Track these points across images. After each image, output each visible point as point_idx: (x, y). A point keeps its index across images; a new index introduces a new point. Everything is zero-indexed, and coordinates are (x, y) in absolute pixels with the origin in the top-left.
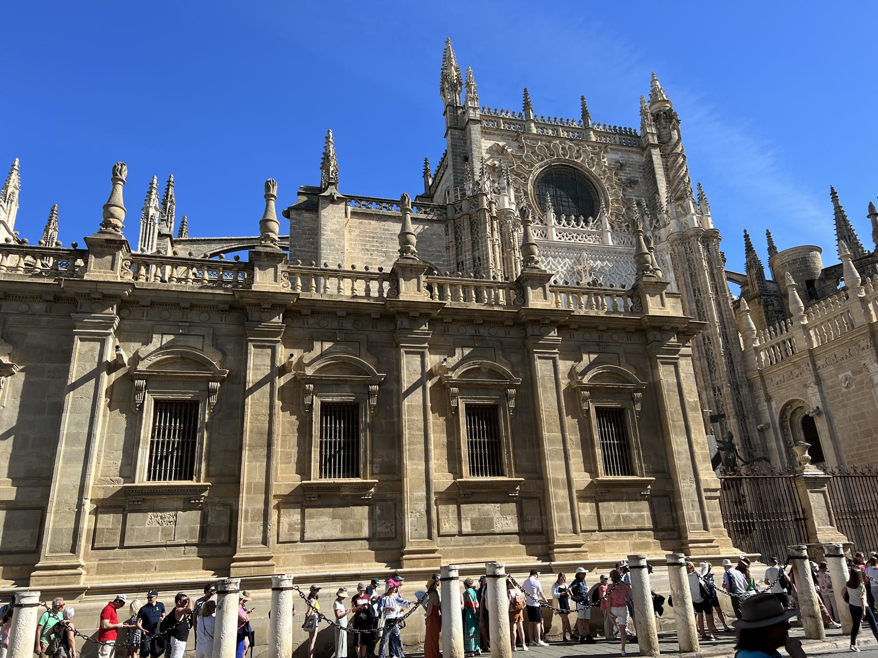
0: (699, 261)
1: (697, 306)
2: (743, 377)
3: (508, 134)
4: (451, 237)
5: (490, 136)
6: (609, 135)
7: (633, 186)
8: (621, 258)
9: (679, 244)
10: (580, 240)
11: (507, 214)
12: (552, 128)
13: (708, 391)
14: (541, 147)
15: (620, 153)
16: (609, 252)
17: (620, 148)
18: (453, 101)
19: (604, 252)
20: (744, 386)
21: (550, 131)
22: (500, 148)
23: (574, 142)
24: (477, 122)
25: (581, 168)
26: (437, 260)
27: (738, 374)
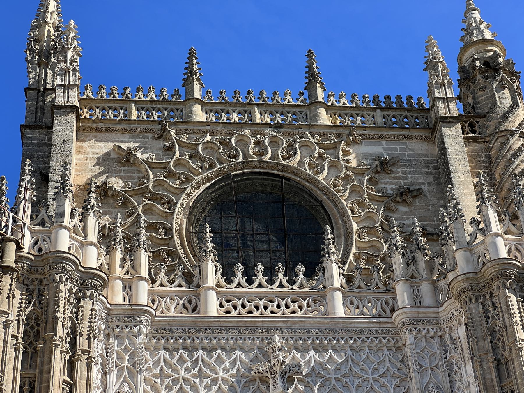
0: (509, 330)
3: (143, 127)
5: (108, 135)
6: (361, 113)
7: (409, 200)
8: (364, 341)
9: (470, 300)
10: (272, 312)
12: (238, 109)
14: (209, 145)
15: (384, 142)
16: (335, 331)
17: (383, 133)
18: (39, 81)
19: (322, 332)
21: (235, 114)
22: (124, 154)
23: (281, 130)
24: (68, 109)
25: (296, 175)
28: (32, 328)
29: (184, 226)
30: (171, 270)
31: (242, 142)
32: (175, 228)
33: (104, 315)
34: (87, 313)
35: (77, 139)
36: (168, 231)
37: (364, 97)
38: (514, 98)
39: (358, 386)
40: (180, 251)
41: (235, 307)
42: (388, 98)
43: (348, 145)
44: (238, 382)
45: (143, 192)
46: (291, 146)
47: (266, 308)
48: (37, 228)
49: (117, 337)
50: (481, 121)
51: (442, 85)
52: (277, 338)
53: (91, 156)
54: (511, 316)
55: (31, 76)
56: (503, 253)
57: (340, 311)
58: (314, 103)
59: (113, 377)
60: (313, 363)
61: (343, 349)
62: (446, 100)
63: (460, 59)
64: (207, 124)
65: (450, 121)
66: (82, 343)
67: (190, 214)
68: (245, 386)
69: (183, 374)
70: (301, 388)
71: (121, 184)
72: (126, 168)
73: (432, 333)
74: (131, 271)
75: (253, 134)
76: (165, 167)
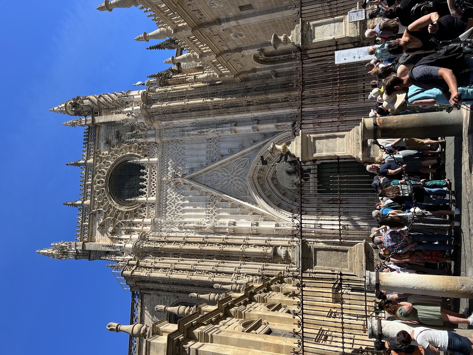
0: (163, 108)
1: (194, 111)
2: (240, 85)
3: (91, 221)
4: (152, 292)
8: (166, 153)
10: (155, 180)
11: (136, 248)
12: (86, 189)
13: (251, 109)
15: (100, 142)
16: (162, 161)
17: (97, 142)
18: (73, 255)
19: (162, 165)
20: (246, 85)
23: (94, 175)
24: (84, 245)
25: (110, 171)
27: (238, 88)
28: (157, 255)
30: (141, 212)
32: (126, 210)
34: (153, 238)
37: (84, 147)
38: (86, 99)
39: (179, 155)
40: (134, 208)
41: (153, 192)
42: (84, 140)
43: (100, 154)
44: (177, 191)
45: (114, 221)
46: (100, 172)
47: (154, 182)
48: (124, 254)
49: (161, 228)
50: (94, 110)
51: (80, 121)
53: (101, 238)
54: (159, 107)
55: (71, 258)
56: (139, 107)
57: (156, 159)
58: (85, 164)
59: (173, 229)
61: (168, 159)
62: (86, 120)
63: (71, 115)
64: (91, 199)
65: (93, 120)
66: (163, 239)
67: (122, 205)
68: (178, 189)
69: (174, 208)
70: (179, 172)
71: (111, 227)
73: (163, 132)
74: (140, 224)
75: (96, 184)
76: (105, 213)
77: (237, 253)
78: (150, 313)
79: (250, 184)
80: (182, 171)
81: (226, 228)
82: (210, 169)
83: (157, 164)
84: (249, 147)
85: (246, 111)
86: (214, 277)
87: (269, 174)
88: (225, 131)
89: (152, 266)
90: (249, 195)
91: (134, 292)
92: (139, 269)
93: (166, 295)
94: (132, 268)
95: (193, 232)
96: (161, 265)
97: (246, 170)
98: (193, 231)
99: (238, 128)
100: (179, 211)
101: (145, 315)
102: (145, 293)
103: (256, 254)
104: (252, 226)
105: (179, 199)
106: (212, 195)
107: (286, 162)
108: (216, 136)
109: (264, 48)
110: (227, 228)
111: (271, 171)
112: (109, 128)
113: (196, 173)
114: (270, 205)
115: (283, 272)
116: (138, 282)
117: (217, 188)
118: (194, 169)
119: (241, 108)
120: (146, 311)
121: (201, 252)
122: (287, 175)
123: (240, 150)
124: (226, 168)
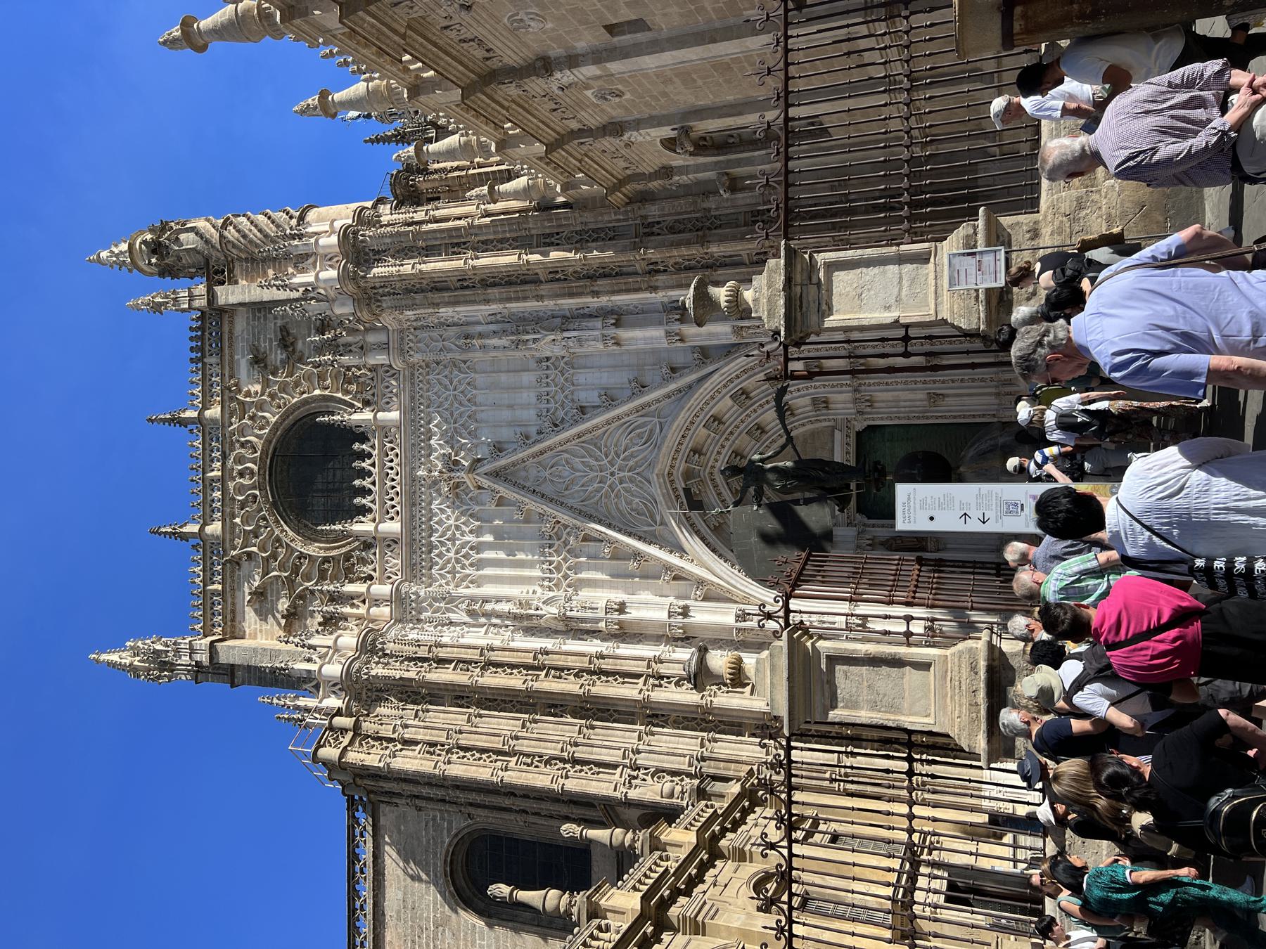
0: (403, 277)
1: (494, 285)
2: (627, 212)
3: (229, 580)
6: (208, 377)
7: (291, 339)
9: (379, 306)
11: (351, 680)
13: (658, 284)
14: (244, 520)
15: (236, 357)
17: (227, 357)
18: (189, 671)
19: (414, 433)
20: (642, 212)
21: (214, 495)
23: (227, 452)
24: (213, 650)
25: (270, 442)
26: (442, 832)
27: (619, 220)
28: (409, 697)
29: (322, 545)
30: (363, 561)
31: (240, 489)
33: (400, 625)
35: (243, 638)
36: (326, 560)
37: (192, 372)
39: (461, 404)
40: (344, 550)
41: (393, 507)
42: (192, 349)
43: (240, 391)
44: (458, 507)
45: (291, 583)
46: (243, 445)
47: (393, 480)
48: (321, 693)
50: (212, 263)
51: (175, 300)
52: (420, 473)
53: (258, 626)
54: (392, 275)
55: (184, 678)
56: (332, 273)
57: (394, 415)
58: (200, 420)
59: (453, 616)
60: (441, 442)
61: (429, 414)
62: (191, 297)
63: (151, 274)
64: (224, 521)
65: (211, 296)
66: (423, 652)
68: (461, 502)
69: (452, 555)
70: (463, 454)
71: (284, 599)
72: (269, 595)
73: (411, 337)
74: (362, 599)
75: (233, 479)
76: (267, 560)
77: (628, 703)
78: (399, 854)
79: (663, 496)
80: (470, 450)
81: (598, 620)
82: (550, 448)
83: (399, 428)
84: (660, 386)
85: (646, 289)
86: (567, 777)
87: (716, 461)
88: (587, 340)
89: (395, 736)
90: (661, 524)
91: (353, 797)
92: (361, 745)
93: (440, 810)
94: (341, 739)
95: (507, 627)
96: (420, 735)
97: (652, 452)
98: (507, 622)
99: (624, 334)
100: (467, 563)
101: (387, 857)
102: (382, 802)
103: (682, 708)
104: (670, 617)
105: (467, 530)
106: (559, 522)
107: (759, 506)
108: (563, 353)
109: (691, 124)
110: (600, 620)
111: (724, 451)
112: (259, 318)
113: (510, 460)
114: (720, 556)
115: (758, 770)
116: (362, 777)
117: (570, 502)
118: (506, 446)
119: (630, 280)
120: (387, 848)
121: (529, 697)
122: (762, 545)
123: (633, 396)
124: (595, 445)
